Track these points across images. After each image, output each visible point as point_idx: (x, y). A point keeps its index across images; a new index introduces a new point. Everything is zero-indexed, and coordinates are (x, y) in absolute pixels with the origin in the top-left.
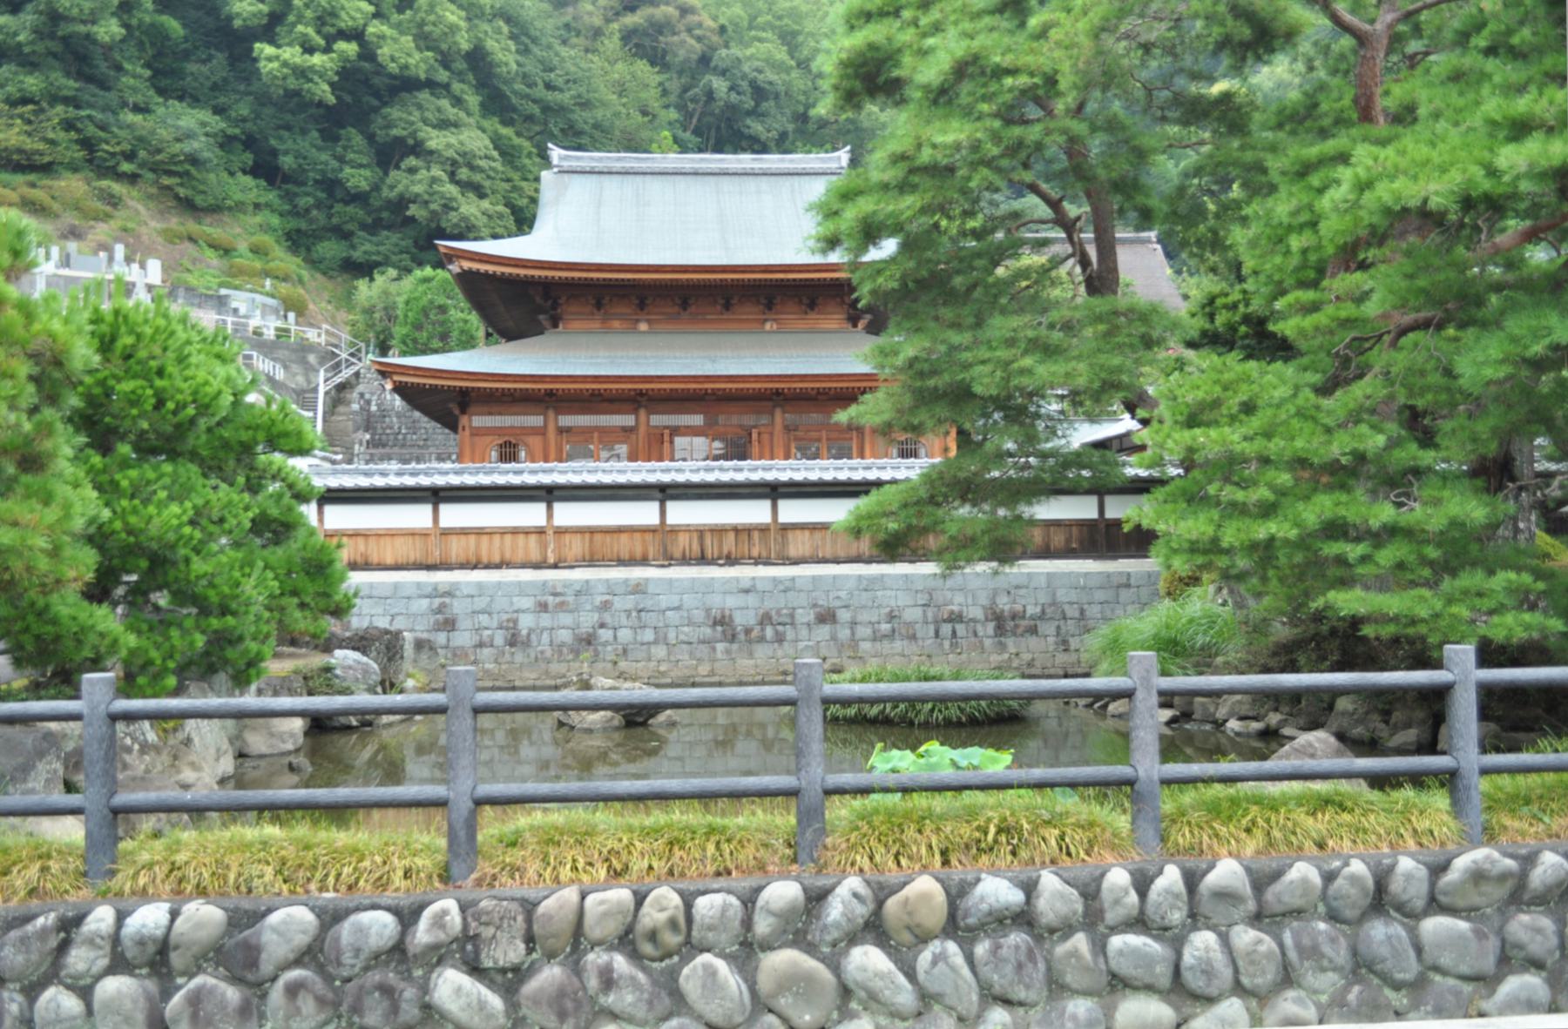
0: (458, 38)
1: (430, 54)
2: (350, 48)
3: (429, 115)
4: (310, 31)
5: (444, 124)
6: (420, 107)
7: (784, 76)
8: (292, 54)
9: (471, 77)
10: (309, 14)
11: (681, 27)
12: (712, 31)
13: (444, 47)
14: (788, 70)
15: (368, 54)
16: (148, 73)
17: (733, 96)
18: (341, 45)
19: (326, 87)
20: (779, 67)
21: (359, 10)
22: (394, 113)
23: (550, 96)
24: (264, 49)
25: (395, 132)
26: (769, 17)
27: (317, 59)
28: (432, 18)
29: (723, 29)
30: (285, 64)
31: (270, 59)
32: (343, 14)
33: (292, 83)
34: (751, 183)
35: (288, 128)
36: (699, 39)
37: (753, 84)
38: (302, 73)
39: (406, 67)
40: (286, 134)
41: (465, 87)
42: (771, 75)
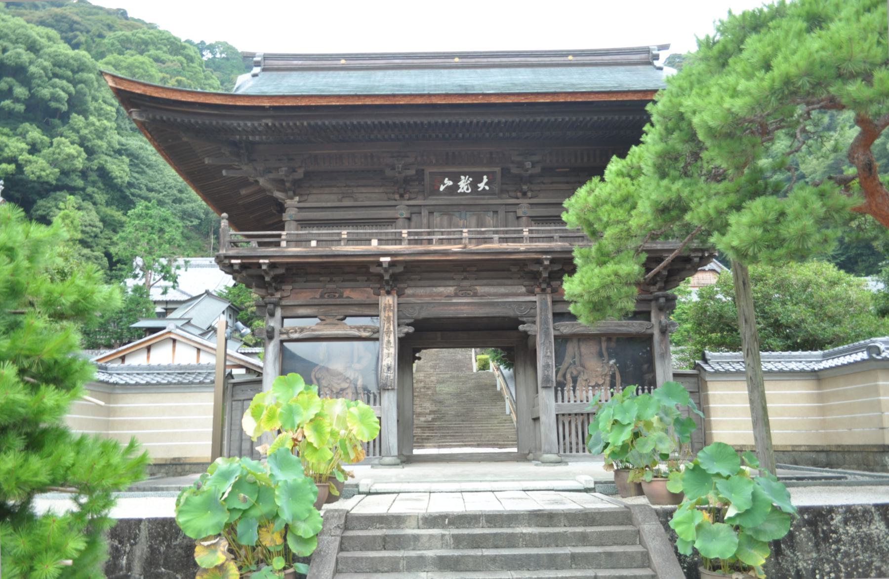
0: (76, 162)
1: (57, 170)
2: (11, 167)
9: (100, 184)
13: (66, 167)
15: (20, 167)
21: (16, 147)
22: (40, 202)
25: (39, 212)
28: (58, 151)
32: (6, 149)
39: (39, 177)
41: (95, 190)
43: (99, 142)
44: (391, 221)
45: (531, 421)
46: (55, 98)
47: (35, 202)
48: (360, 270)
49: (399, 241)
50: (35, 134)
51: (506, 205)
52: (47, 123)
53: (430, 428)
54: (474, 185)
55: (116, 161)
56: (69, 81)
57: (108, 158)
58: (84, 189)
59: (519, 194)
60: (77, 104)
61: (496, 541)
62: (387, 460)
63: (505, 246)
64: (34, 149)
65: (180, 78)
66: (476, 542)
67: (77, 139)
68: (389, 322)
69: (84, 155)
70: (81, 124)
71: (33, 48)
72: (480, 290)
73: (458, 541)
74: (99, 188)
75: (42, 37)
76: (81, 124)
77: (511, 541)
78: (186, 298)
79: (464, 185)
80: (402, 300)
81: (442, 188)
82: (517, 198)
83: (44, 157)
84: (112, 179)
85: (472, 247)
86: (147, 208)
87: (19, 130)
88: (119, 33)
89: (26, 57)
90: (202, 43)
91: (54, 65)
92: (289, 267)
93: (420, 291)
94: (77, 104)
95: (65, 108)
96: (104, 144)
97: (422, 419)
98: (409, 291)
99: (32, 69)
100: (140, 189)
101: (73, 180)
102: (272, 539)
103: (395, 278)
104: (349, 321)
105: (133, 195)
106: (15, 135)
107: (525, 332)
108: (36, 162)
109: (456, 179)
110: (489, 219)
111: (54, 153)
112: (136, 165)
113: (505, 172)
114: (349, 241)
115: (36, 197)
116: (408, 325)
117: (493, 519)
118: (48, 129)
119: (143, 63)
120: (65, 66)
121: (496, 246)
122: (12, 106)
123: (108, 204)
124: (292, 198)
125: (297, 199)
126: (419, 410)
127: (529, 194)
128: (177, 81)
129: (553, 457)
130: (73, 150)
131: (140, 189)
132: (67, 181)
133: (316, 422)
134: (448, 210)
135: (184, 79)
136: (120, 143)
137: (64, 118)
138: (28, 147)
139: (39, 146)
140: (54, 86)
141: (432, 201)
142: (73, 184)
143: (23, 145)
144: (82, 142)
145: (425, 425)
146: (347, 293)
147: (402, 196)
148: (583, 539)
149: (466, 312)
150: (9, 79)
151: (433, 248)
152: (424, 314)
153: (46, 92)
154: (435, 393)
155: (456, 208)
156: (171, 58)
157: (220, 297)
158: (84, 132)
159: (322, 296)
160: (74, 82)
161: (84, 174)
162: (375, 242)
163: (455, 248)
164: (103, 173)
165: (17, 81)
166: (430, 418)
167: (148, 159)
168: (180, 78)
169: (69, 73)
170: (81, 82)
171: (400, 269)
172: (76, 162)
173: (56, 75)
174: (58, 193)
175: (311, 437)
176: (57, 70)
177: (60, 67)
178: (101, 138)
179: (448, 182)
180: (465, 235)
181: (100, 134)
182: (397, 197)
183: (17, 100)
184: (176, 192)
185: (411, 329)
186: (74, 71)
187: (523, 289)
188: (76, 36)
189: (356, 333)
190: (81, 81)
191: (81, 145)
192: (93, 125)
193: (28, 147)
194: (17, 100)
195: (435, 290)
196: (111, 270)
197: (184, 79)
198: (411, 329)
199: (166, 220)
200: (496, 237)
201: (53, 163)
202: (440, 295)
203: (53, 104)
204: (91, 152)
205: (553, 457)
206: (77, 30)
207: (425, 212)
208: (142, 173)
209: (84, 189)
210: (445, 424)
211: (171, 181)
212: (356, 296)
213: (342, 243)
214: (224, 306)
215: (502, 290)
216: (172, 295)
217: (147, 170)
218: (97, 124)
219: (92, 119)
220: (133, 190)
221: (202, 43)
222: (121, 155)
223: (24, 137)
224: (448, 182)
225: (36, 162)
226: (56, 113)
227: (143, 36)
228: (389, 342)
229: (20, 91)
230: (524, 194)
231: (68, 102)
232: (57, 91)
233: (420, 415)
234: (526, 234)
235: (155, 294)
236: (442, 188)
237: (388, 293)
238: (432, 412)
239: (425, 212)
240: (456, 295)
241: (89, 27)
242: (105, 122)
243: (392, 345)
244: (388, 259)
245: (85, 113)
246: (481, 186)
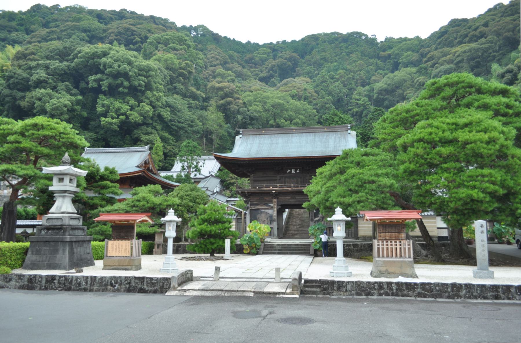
0: (149, 113)
3: (143, 131)
4: (113, 114)
5: (147, 134)
6: (141, 130)
7: (259, 114)
8: (109, 120)
9: (158, 121)
10: (113, 110)
11: (234, 103)
12: (241, 104)
13: (146, 115)
14: (261, 112)
15: (127, 117)
16: (80, 125)
17: (244, 120)
18: (121, 117)
19: (116, 127)
20: (259, 112)
21: (126, 108)
22: (136, 131)
23: (180, 125)
24: (103, 119)
25: (135, 136)
26: (260, 99)
27: (114, 120)
29: (244, 103)
30: (106, 122)
31: (103, 121)
32: (122, 110)
33: (108, 126)
34: (126, 154)
35: (113, 136)
36: (238, 106)
37: (250, 116)
38: (111, 124)
39: (136, 121)
40: (113, 137)
42: (255, 114)
43: (158, 103)
44: (276, 180)
46: (140, 85)
47: (133, 131)
48: (269, 193)
50: (132, 101)
52: (135, 94)
53: (298, 231)
54: (296, 171)
55: (164, 110)
56: (145, 77)
57: (162, 110)
58: (152, 124)
60: (148, 87)
61: (288, 248)
64: (132, 108)
65: (187, 62)
66: (285, 248)
67: (149, 102)
69: (152, 110)
70: (151, 96)
71: (130, 63)
72: (297, 197)
73: (282, 247)
74: (158, 123)
75: (132, 57)
76: (151, 96)
77: (290, 248)
78: (204, 177)
79: (293, 171)
83: (136, 111)
84: (163, 118)
85: (294, 189)
86: (189, 143)
87: (126, 100)
88: (156, 35)
89: (128, 68)
90: (191, 26)
91: (139, 70)
92: (252, 193)
93: (282, 198)
94: (148, 87)
95: (143, 89)
96: (159, 104)
99: (131, 73)
100: (175, 122)
101: (147, 120)
102: (254, 246)
103: (276, 195)
105: (172, 125)
106: (125, 102)
108: (134, 114)
109: (291, 170)
110: (299, 180)
111: (141, 110)
112: (173, 111)
114: (266, 187)
115: (133, 129)
117: (288, 245)
118: (135, 97)
119: (171, 58)
120: (143, 70)
122: (123, 90)
123: (162, 130)
126: (294, 224)
128: (186, 63)
130: (148, 108)
131: (175, 122)
132: (145, 121)
133: (260, 229)
135: (188, 62)
136: (166, 102)
137: (143, 93)
138: (130, 108)
139: (134, 106)
140: (139, 80)
141: (286, 175)
142: (148, 122)
143: (128, 107)
144: (151, 104)
146: (265, 198)
148: (302, 248)
149: (293, 203)
150: (122, 79)
152: (283, 203)
153: (136, 83)
156: (180, 47)
157: (217, 177)
158: (152, 99)
160: (146, 77)
161: (152, 118)
163: (290, 189)
164: (160, 116)
165: (125, 79)
166: (298, 227)
167: (177, 107)
168: (187, 62)
169: (145, 73)
170: (150, 76)
172: (149, 113)
173: (139, 75)
174: (142, 127)
175: (259, 231)
176: (140, 72)
177: (141, 71)
178: (158, 101)
179: (289, 171)
181: (158, 100)
183: (125, 88)
184: (190, 122)
186: (145, 71)
188: (135, 38)
190: (150, 76)
191: (151, 105)
192: (155, 95)
193: (130, 108)
194: (125, 88)
196: (165, 160)
197: (188, 62)
199: (195, 147)
201: (141, 114)
203: (139, 88)
204: (154, 107)
206: (135, 35)
207: (284, 178)
208: (175, 114)
209: (152, 124)
210: (303, 229)
211: (188, 117)
214: (218, 181)
215: (302, 197)
216: (198, 176)
217: (177, 113)
218: (157, 94)
219: (155, 93)
220: (172, 123)
221: (191, 26)
222: (166, 107)
223: (128, 103)
224: (289, 171)
225: (134, 114)
226: (140, 91)
227: (166, 37)
229: (126, 83)
231: (146, 86)
232: (141, 81)
235: (192, 176)
238: (299, 225)
239: (284, 178)
241: (140, 33)
242: (160, 94)
245: (151, 89)
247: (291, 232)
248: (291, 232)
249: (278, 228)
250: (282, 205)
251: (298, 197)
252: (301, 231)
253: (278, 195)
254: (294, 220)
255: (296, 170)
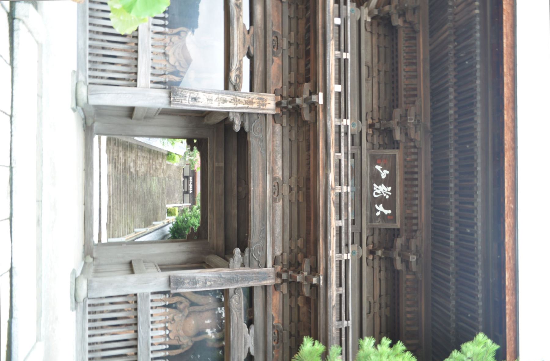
45: (128, 259)
49: (342, 114)
51: (361, 234)
53: (124, 170)
54: (381, 200)
59: (371, 247)
62: (83, 90)
63: (333, 233)
68: (246, 103)
72: (279, 205)
79: (382, 190)
80: (270, 119)
81: (378, 168)
82: (367, 245)
85: (333, 196)
93: (278, 140)
97: (132, 165)
98: (278, 127)
104: (246, 62)
107: (232, 255)
109: (390, 181)
113: (395, 233)
116: (242, 128)
121: (334, 223)
124: (369, 14)
125: (369, 20)
126: (139, 162)
127: (371, 257)
129: (83, 293)
134: (357, 173)
145: (127, 166)
146: (277, 61)
147: (371, 126)
151: (332, 151)
154: (152, 176)
155: (361, 181)
159: (274, 32)
162: (338, 88)
166: (132, 170)
171: (306, 116)
179: (384, 174)
180: (344, 189)
182: (370, 121)
185: (237, 128)
187: (278, 253)
189: (235, 65)
195: (279, 156)
198: (237, 128)
200: (342, 223)
202: (274, 162)
205: (83, 293)
210: (127, 181)
212: (274, 69)
213: (338, 53)
215: (278, 229)
224: (384, 174)
228: (225, 101)
230: (372, 252)
233: (135, 162)
234: (345, 256)
236: (378, 168)
237: (278, 104)
238: (137, 172)
240: (274, 179)
243: (222, 105)
244: (321, 102)
246: (380, 208)
247: (121, 155)
248: (121, 155)
249: (131, 111)
250: (243, 134)
251: (279, 212)
252: (124, 178)
253: (300, 120)
254: (146, 162)
255: (389, 203)
